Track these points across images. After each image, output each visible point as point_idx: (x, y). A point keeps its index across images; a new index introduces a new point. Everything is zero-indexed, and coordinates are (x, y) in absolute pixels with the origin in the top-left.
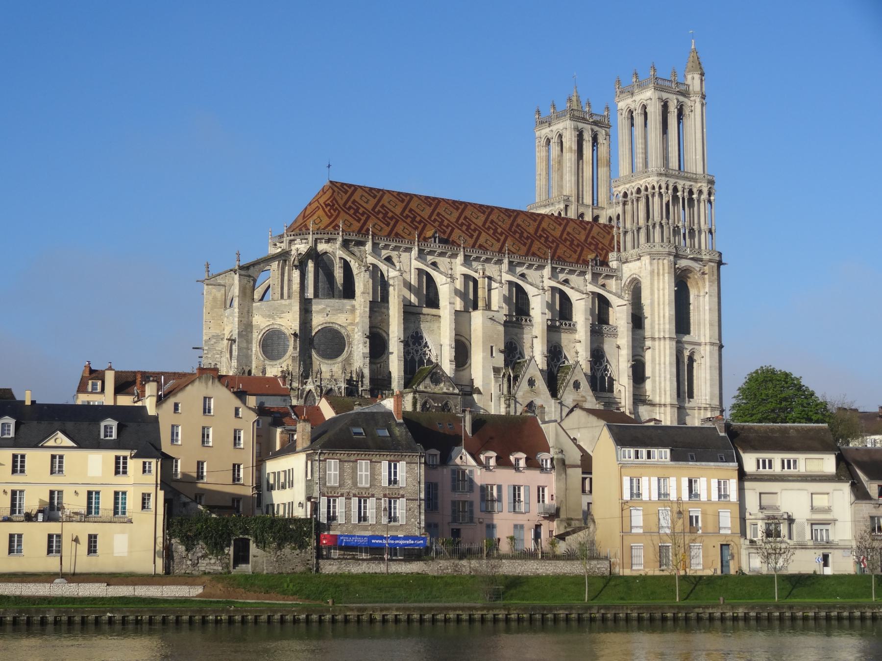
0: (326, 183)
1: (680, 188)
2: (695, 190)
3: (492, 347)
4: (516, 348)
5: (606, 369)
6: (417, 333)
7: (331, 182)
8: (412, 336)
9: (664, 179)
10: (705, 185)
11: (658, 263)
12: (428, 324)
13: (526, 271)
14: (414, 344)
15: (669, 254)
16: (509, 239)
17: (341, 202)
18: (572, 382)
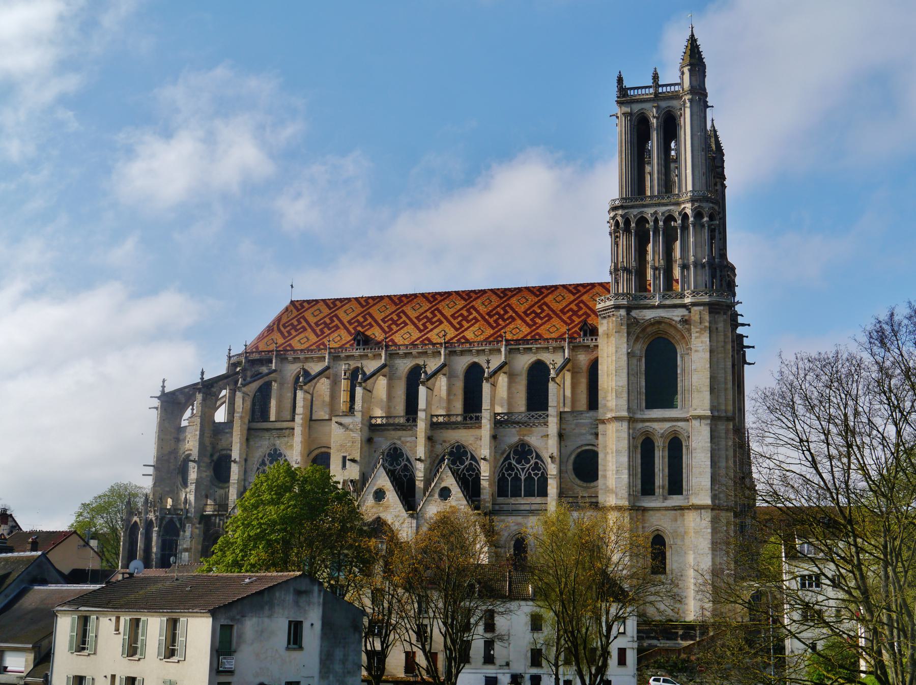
0: (288, 303)
1: (649, 217)
2: (676, 215)
3: (344, 458)
4: (465, 453)
5: (536, 467)
6: (275, 450)
7: (292, 302)
8: (270, 455)
9: (620, 212)
10: (689, 205)
11: (608, 323)
12: (286, 439)
13: (476, 360)
14: (271, 463)
15: (617, 307)
16: (477, 325)
17: (284, 320)
18: (437, 491)
